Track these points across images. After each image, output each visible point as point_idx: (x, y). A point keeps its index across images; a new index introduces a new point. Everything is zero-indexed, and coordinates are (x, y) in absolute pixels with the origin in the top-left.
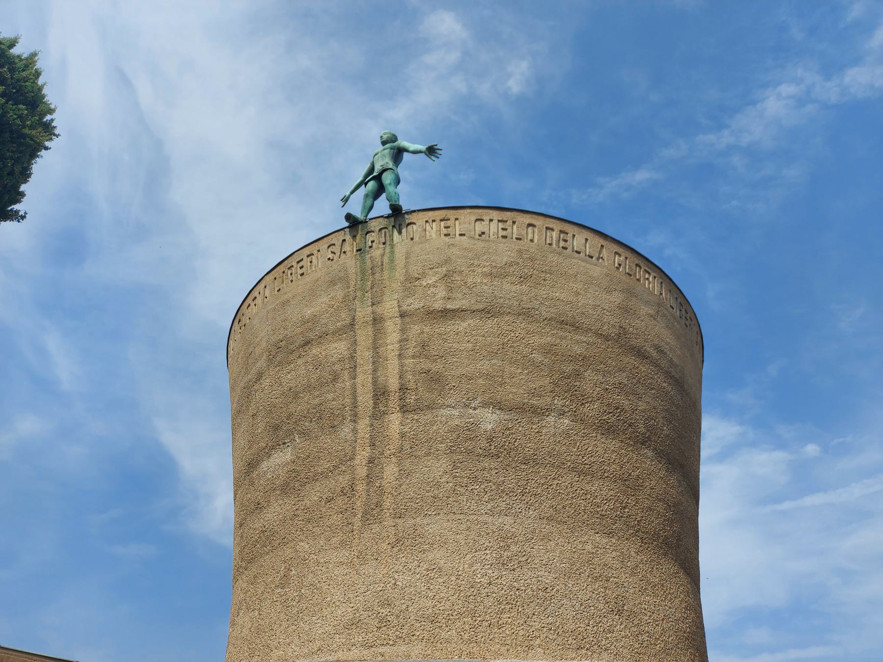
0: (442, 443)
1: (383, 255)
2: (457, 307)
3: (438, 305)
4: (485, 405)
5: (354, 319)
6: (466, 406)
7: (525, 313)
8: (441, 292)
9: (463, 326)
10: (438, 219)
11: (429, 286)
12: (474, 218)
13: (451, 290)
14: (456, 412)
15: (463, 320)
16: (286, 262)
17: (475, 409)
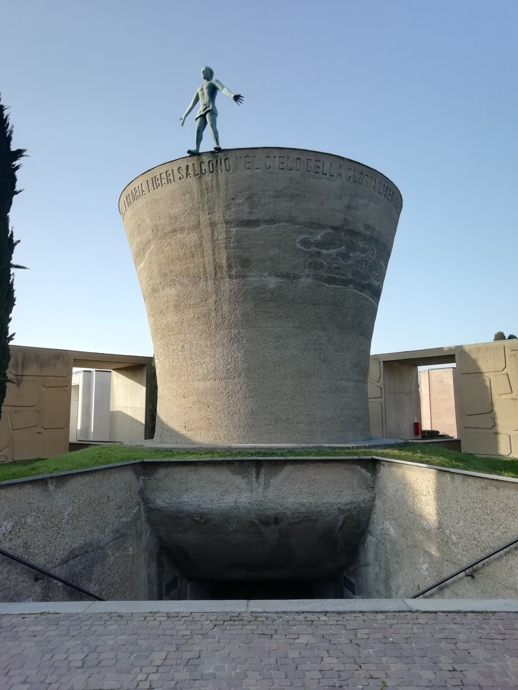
1: (212, 181)
2: (256, 218)
3: (245, 217)
4: (271, 275)
5: (199, 222)
7: (292, 221)
8: (247, 209)
10: (243, 157)
13: (252, 207)
14: (256, 279)
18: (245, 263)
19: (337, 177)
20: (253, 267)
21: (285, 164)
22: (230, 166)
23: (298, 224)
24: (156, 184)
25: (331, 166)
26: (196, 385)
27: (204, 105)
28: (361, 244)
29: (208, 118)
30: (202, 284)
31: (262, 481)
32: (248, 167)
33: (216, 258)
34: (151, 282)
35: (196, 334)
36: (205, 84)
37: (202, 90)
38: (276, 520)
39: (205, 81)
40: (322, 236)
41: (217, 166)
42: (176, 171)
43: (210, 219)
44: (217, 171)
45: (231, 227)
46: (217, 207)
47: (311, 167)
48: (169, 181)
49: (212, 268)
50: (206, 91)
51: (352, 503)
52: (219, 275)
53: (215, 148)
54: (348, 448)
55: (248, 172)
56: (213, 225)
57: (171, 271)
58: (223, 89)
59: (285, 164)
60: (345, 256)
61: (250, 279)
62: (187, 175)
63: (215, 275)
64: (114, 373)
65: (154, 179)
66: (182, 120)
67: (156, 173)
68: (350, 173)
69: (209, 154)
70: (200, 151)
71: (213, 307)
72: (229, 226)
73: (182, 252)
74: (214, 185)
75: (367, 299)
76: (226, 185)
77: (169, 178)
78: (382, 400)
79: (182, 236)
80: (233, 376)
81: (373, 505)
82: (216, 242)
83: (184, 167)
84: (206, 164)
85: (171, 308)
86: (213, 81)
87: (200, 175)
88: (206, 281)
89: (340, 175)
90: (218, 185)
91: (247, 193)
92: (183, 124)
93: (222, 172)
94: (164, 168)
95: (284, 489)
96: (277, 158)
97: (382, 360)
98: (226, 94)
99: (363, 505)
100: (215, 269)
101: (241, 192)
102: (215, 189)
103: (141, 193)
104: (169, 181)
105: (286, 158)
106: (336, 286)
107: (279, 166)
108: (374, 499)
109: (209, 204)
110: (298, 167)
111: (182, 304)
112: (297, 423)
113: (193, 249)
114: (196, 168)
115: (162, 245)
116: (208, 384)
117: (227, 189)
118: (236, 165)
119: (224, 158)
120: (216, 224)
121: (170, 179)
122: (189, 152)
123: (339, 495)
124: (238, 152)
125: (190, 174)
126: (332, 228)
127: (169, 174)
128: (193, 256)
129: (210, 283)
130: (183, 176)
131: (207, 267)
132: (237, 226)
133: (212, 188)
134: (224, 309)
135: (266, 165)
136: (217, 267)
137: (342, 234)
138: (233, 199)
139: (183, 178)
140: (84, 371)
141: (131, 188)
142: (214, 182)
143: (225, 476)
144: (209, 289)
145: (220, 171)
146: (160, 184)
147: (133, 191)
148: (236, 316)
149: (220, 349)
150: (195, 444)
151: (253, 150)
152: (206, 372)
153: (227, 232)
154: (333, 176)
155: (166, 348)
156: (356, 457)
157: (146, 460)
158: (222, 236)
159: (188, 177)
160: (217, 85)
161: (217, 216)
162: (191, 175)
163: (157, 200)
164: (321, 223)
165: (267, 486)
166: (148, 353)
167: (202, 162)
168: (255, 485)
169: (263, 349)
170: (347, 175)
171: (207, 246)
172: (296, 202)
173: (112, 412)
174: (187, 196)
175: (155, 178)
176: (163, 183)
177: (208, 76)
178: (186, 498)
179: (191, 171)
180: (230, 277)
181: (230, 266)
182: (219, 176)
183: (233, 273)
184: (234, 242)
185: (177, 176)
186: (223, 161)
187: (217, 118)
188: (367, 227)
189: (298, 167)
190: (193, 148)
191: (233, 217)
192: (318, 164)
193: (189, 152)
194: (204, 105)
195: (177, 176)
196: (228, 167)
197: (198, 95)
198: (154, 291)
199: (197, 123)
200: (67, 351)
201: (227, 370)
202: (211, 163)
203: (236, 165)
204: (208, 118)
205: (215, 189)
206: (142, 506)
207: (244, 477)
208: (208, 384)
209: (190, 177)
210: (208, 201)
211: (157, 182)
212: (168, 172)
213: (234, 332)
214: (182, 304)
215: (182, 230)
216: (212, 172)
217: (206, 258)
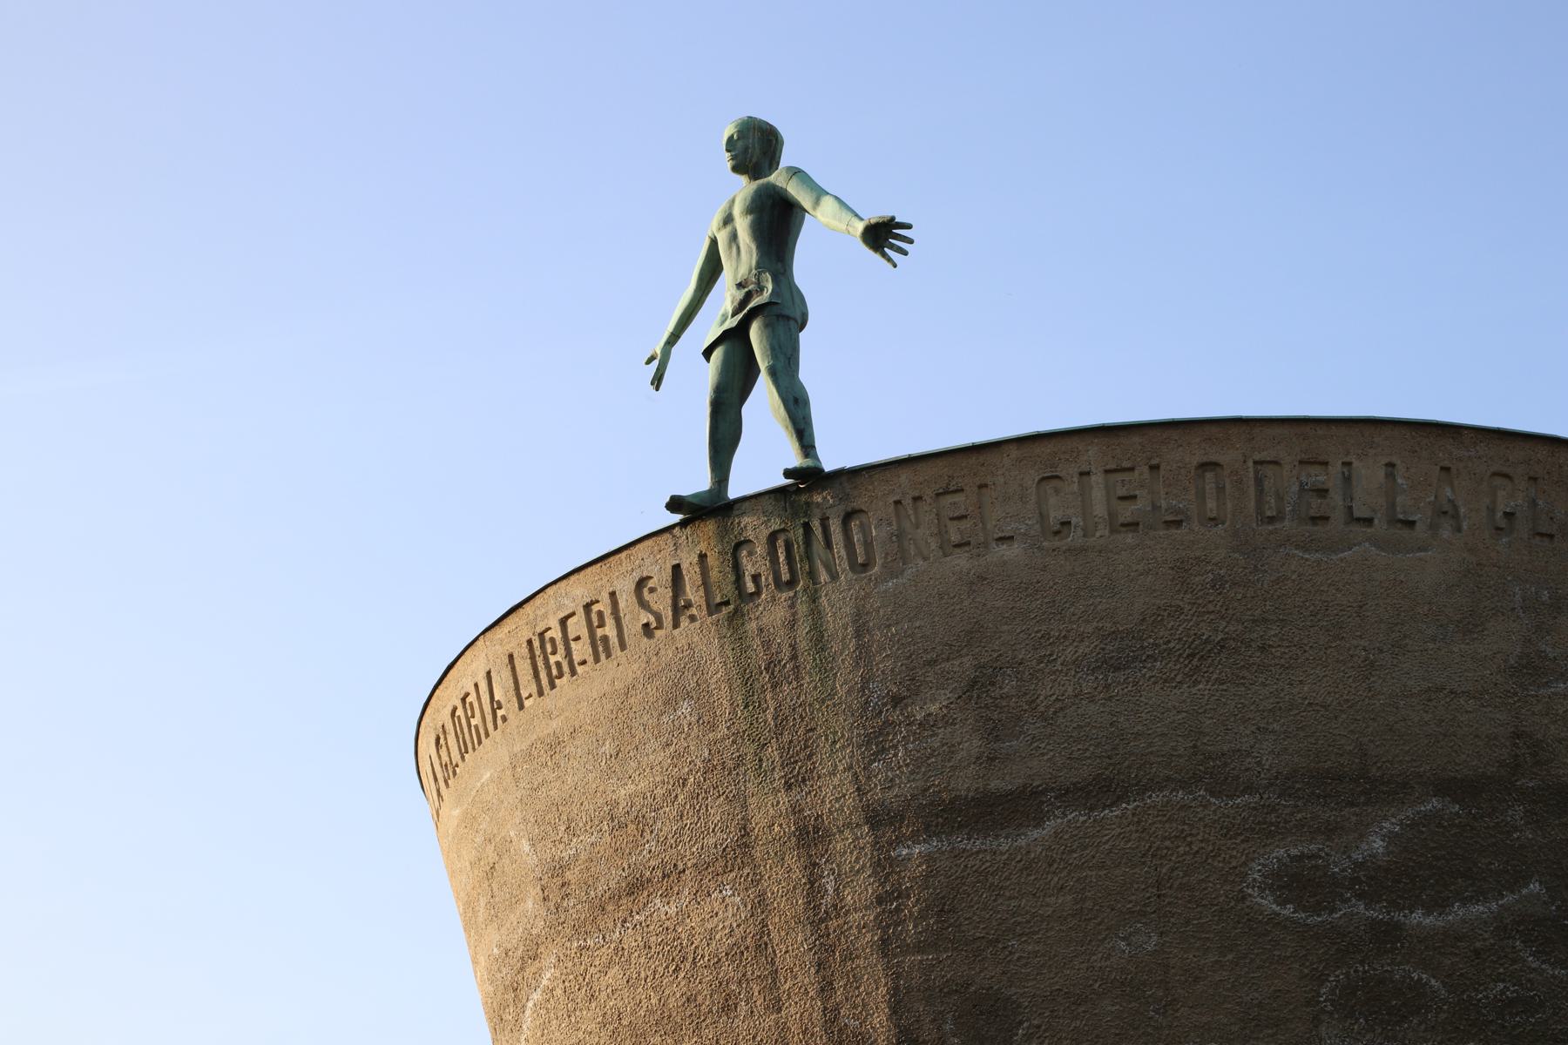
1: (792, 624)
3: (965, 783)
5: (745, 831)
8: (972, 745)
9: (1036, 837)
10: (928, 494)
11: (928, 724)
15: (1039, 824)
16: (528, 608)
19: (1434, 527)
21: (1142, 504)
22: (868, 544)
23: (1249, 789)
24: (548, 667)
25: (1390, 476)
27: (740, 286)
29: (760, 341)
32: (955, 537)
33: (837, 1009)
36: (742, 188)
37: (728, 220)
39: (743, 180)
40: (1391, 838)
41: (808, 556)
42: (626, 601)
43: (796, 810)
44: (812, 575)
45: (899, 841)
46: (824, 747)
47: (1280, 498)
50: (742, 225)
53: (788, 473)
55: (961, 561)
56: (810, 836)
58: (817, 202)
59: (1142, 504)
62: (677, 611)
65: (539, 646)
66: (655, 363)
67: (545, 616)
68: (1509, 498)
69: (768, 504)
70: (734, 491)
72: (890, 834)
73: (675, 991)
74: (803, 645)
76: (858, 634)
77: (600, 632)
79: (672, 910)
82: (833, 924)
83: (661, 578)
84: (760, 549)
86: (776, 178)
87: (733, 605)
90: (819, 640)
92: (657, 381)
93: (834, 577)
94: (578, 592)
96: (1097, 479)
98: (834, 223)
101: (932, 663)
102: (807, 661)
103: (489, 718)
104: (600, 647)
105: (1143, 472)
107: (1112, 515)
109: (786, 738)
110: (1211, 504)
113: (727, 969)
114: (714, 574)
115: (585, 960)
117: (863, 655)
118: (900, 535)
119: (841, 509)
120: (828, 835)
121: (605, 639)
122: (675, 504)
124: (904, 477)
125: (688, 605)
126: (1444, 787)
127: (600, 614)
128: (728, 1008)
132: (929, 830)
133: (794, 657)
135: (1043, 517)
137: (1517, 813)
138: (897, 701)
141: (449, 696)
142: (803, 629)
145: (824, 576)
146: (566, 668)
147: (460, 712)
151: (973, 459)
153: (884, 866)
154: (1411, 524)
158: (860, 892)
159: (684, 622)
160: (795, 191)
161: (828, 793)
162: (694, 611)
163: (554, 745)
167: (738, 546)
170: (1492, 510)
171: (793, 945)
174: (685, 708)
175: (542, 643)
176: (577, 658)
177: (756, 152)
179: (693, 593)
182: (824, 601)
184: (923, 915)
185: (635, 618)
186: (835, 527)
187: (804, 336)
189: (1211, 504)
190: (697, 481)
191: (906, 788)
192: (1317, 476)
193: (675, 504)
194: (740, 286)
195: (635, 618)
196: (859, 550)
197: (714, 242)
199: (707, 374)
202: (780, 543)
203: (900, 535)
204: (760, 341)
205: (807, 661)
209: (693, 618)
210: (781, 723)
211: (552, 659)
212: (595, 608)
215: (671, 874)
216: (791, 583)
217: (792, 1010)
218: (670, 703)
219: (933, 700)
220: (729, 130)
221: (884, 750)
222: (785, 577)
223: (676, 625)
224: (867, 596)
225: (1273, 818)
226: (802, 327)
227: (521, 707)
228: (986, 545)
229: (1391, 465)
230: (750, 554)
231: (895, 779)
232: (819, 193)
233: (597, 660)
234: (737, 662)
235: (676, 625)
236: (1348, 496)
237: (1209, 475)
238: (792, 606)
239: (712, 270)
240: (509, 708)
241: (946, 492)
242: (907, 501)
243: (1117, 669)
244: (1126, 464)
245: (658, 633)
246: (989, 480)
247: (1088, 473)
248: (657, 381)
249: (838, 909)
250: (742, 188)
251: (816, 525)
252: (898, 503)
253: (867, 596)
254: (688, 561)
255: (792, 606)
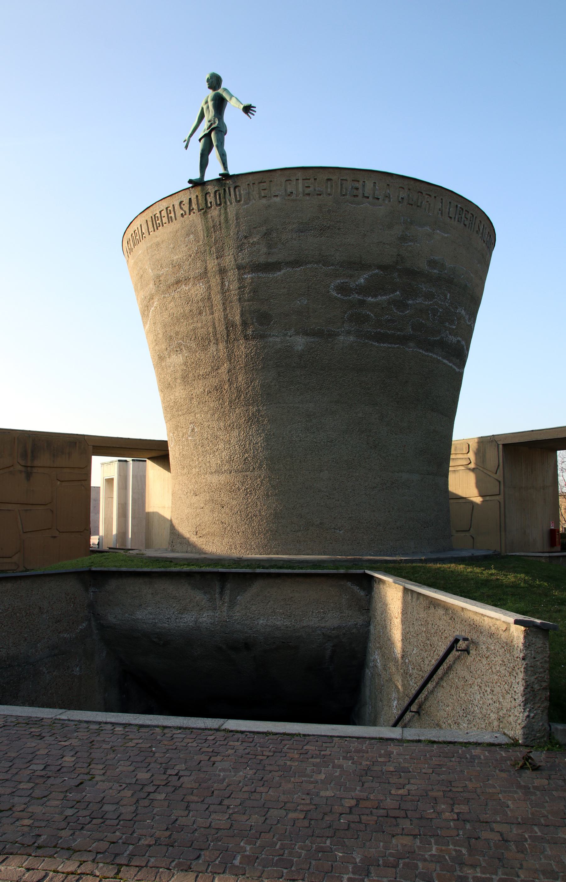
0: (270, 361)
1: (220, 216)
2: (276, 260)
3: (262, 260)
4: (297, 333)
5: (206, 269)
6: (285, 335)
8: (264, 250)
9: (279, 274)
10: (257, 182)
12: (283, 180)
13: (270, 247)
14: (278, 340)
15: (280, 271)
16: (151, 208)
17: (291, 337)
18: (264, 318)
19: (384, 200)
20: (274, 323)
21: (311, 189)
22: (240, 195)
23: (333, 265)
25: (374, 186)
26: (209, 479)
27: (209, 121)
28: (424, 288)
29: (214, 138)
30: (213, 348)
31: (227, 598)
32: (263, 195)
33: (227, 315)
34: (157, 348)
35: (207, 413)
36: (210, 93)
37: (207, 102)
38: (247, 645)
39: (211, 91)
40: (366, 279)
41: (225, 198)
42: (177, 207)
43: (219, 264)
44: (225, 203)
45: (245, 274)
46: (227, 248)
47: (346, 190)
48: (170, 219)
49: (224, 327)
50: (210, 104)
51: (339, 627)
52: (232, 336)
53: (220, 175)
54: (394, 562)
55: (264, 201)
56: (222, 271)
57: (177, 333)
58: (231, 99)
59: (311, 189)
60: (401, 305)
61: (271, 339)
62: (190, 210)
63: (228, 336)
64: (149, 463)
65: (154, 218)
66: (186, 142)
67: (156, 210)
69: (215, 183)
71: (226, 377)
72: (242, 272)
73: (187, 309)
74: (222, 221)
75: (439, 361)
76: (237, 219)
77: (170, 215)
78: (500, 498)
79: (187, 288)
80: (251, 468)
81: (369, 631)
82: (227, 294)
83: (186, 201)
84: (212, 195)
85: (179, 381)
86: (220, 91)
87: (205, 210)
88: (217, 344)
89: (388, 197)
90: (227, 220)
91: (264, 229)
92: (186, 147)
93: (231, 203)
94: (164, 204)
95: (254, 608)
96: (300, 181)
97: (501, 443)
98: (235, 105)
99: (354, 631)
100: (227, 328)
102: (223, 226)
103: (141, 237)
104: (170, 219)
105: (312, 180)
106: (389, 346)
108: (368, 624)
110: (329, 190)
111: (191, 375)
112: (334, 528)
113: (200, 304)
114: (200, 201)
115: (165, 300)
116: (223, 478)
117: (238, 225)
118: (249, 193)
120: (227, 271)
121: (171, 217)
122: (190, 181)
123: (323, 618)
124: (250, 177)
125: (193, 209)
126: (380, 267)
127: (170, 210)
128: (200, 313)
129: (221, 346)
130: (185, 212)
131: (217, 326)
132: (252, 271)
133: (220, 224)
134: (240, 379)
135: (286, 190)
136: (229, 325)
137: (396, 275)
138: (246, 237)
139: (185, 214)
140: (119, 461)
141: (131, 231)
142: (223, 217)
143: (185, 591)
144: (221, 354)
145: (228, 203)
147: (133, 235)
148: (254, 388)
149: (235, 433)
150: (205, 553)
152: (219, 462)
153: (241, 280)
154: (378, 199)
155: (176, 432)
156: (342, 571)
157: (93, 569)
158: (234, 286)
159: (192, 214)
162: (194, 211)
163: (158, 245)
164: (363, 262)
165: (232, 604)
166: (165, 438)
167: (207, 194)
168: (218, 603)
169: (290, 432)
170: (398, 197)
171: (217, 299)
172: (327, 237)
173: (148, 513)
174: (192, 236)
175: (155, 218)
176: (164, 222)
178: (140, 615)
179: (194, 206)
180: (246, 338)
181: (245, 324)
183: (250, 332)
185: (179, 212)
187: (226, 137)
188: (432, 263)
189: (329, 190)
190: (196, 175)
191: (247, 260)
192: (356, 185)
193: (190, 181)
194: (209, 121)
195: (179, 212)
196: (238, 197)
197: (203, 109)
198: (161, 358)
200: (84, 436)
201: (245, 460)
202: (217, 193)
204: (214, 138)
205: (223, 226)
206: (93, 623)
207: (205, 593)
208: (223, 478)
209: (194, 213)
211: (157, 222)
212: (169, 209)
213: (253, 409)
214: (191, 375)
215: (187, 279)
216: (220, 205)
217: (216, 315)
218: (188, 235)
219: (255, 238)
220: (208, 76)
221: (242, 250)
222: (218, 203)
223: (190, 214)
224: (239, 209)
225: (337, 272)
226: (225, 134)
227: (149, 234)
228: (271, 197)
229: (375, 183)
230: (210, 196)
231: (244, 258)
232: (231, 96)
233: (169, 223)
234: (205, 225)
235: (190, 214)
236: (364, 190)
237: (329, 182)
238: (220, 211)
239: (202, 116)
240: (146, 234)
241: (261, 182)
242: (251, 184)
243: (302, 232)
244: (308, 178)
245: (185, 216)
246: (272, 180)
247: (298, 180)
248: (186, 147)
249: (228, 290)
250: (210, 93)
251: (227, 189)
252: (248, 184)
253: (239, 209)
254: (193, 198)
255: (220, 211)
